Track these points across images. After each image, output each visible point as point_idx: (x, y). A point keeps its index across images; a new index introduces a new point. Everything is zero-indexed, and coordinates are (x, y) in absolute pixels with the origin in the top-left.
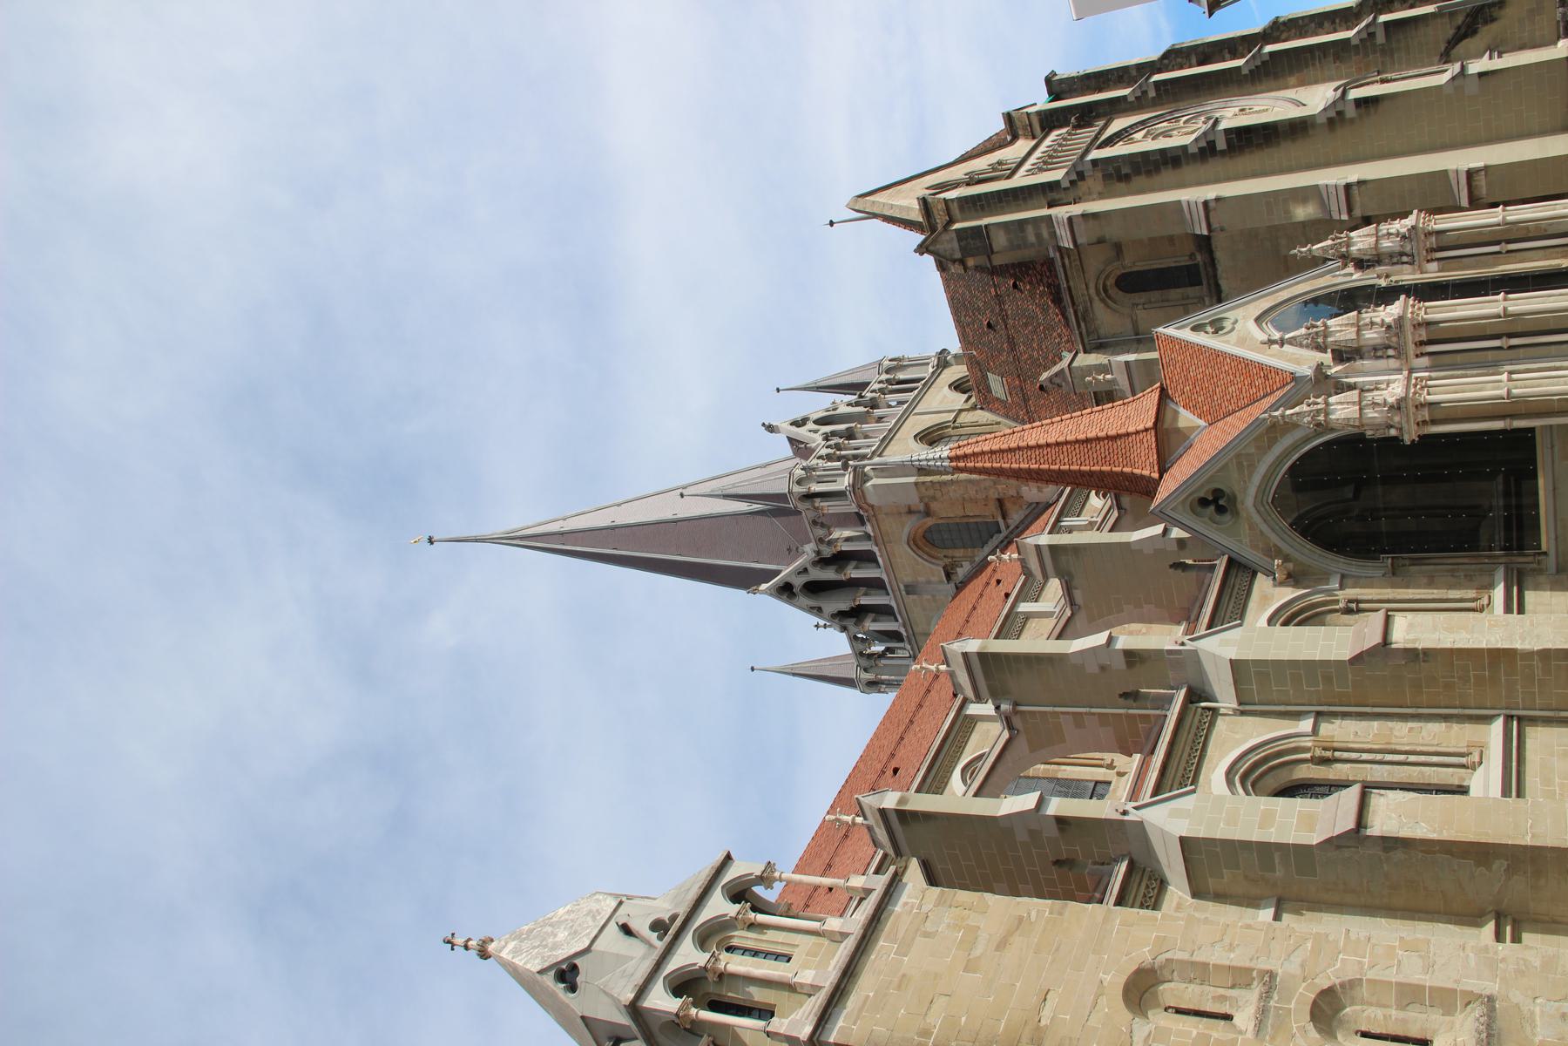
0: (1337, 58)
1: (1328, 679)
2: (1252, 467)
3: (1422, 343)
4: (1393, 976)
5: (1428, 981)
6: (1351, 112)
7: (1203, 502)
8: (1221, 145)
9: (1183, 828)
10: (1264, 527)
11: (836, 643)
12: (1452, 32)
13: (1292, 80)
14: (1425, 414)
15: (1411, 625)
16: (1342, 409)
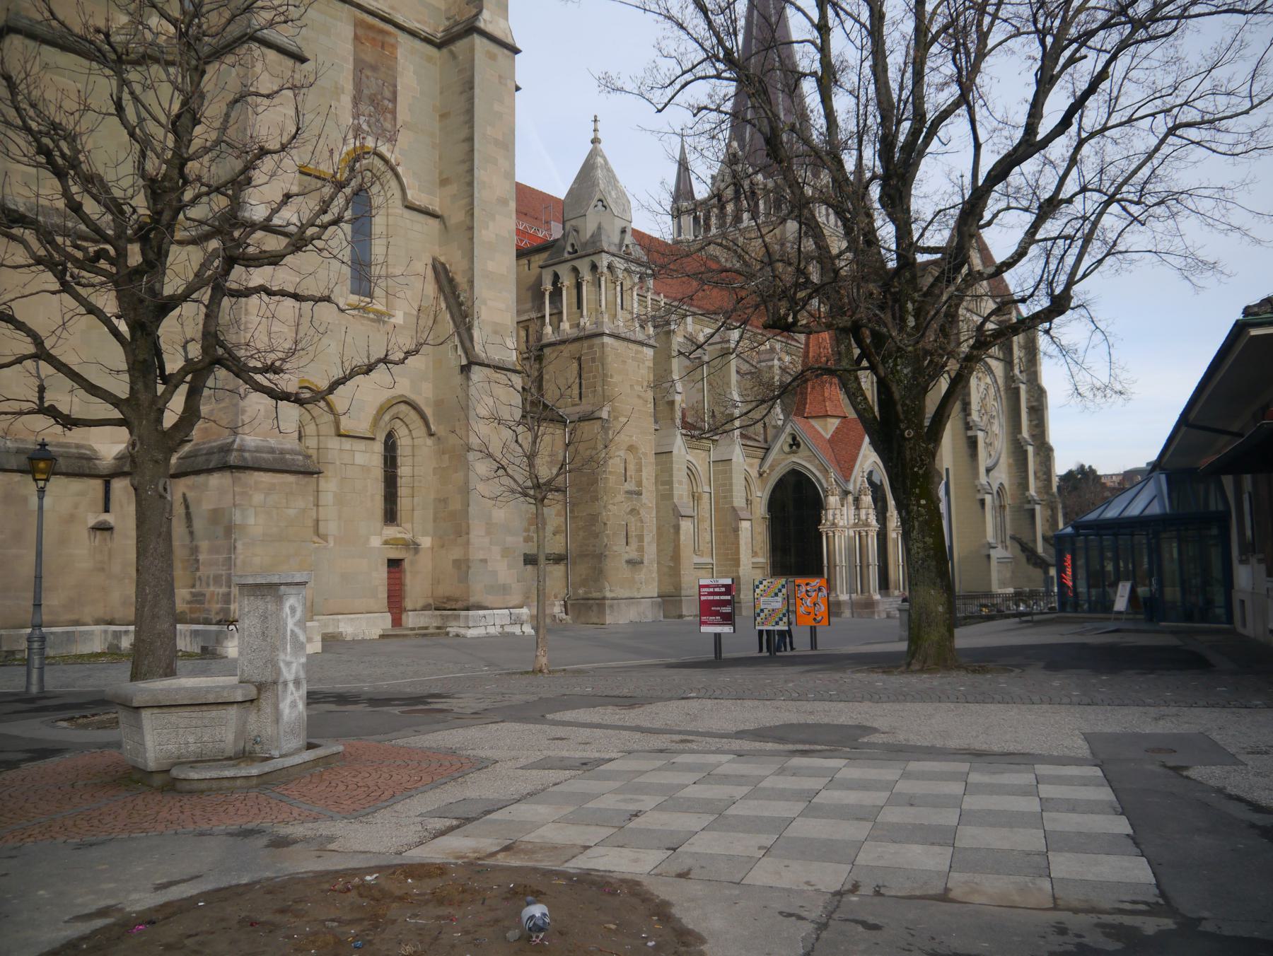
0: (1020, 484)
1: (725, 497)
2: (810, 462)
3: (860, 533)
4: (645, 533)
5: (645, 544)
6: (979, 496)
7: (794, 438)
8: (970, 433)
9: (675, 452)
10: (781, 466)
11: (701, 191)
12: (1025, 540)
13: (1011, 461)
14: (831, 534)
15: (746, 529)
16: (833, 500)
